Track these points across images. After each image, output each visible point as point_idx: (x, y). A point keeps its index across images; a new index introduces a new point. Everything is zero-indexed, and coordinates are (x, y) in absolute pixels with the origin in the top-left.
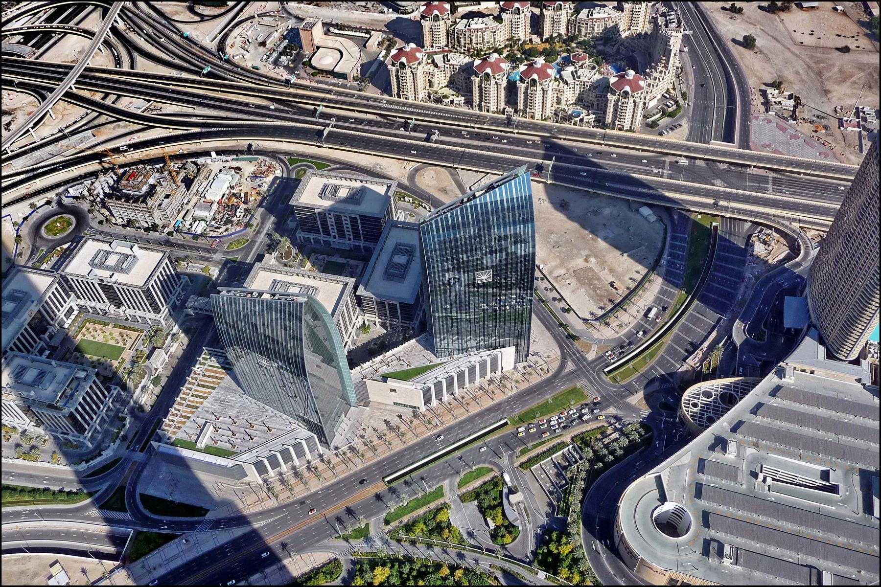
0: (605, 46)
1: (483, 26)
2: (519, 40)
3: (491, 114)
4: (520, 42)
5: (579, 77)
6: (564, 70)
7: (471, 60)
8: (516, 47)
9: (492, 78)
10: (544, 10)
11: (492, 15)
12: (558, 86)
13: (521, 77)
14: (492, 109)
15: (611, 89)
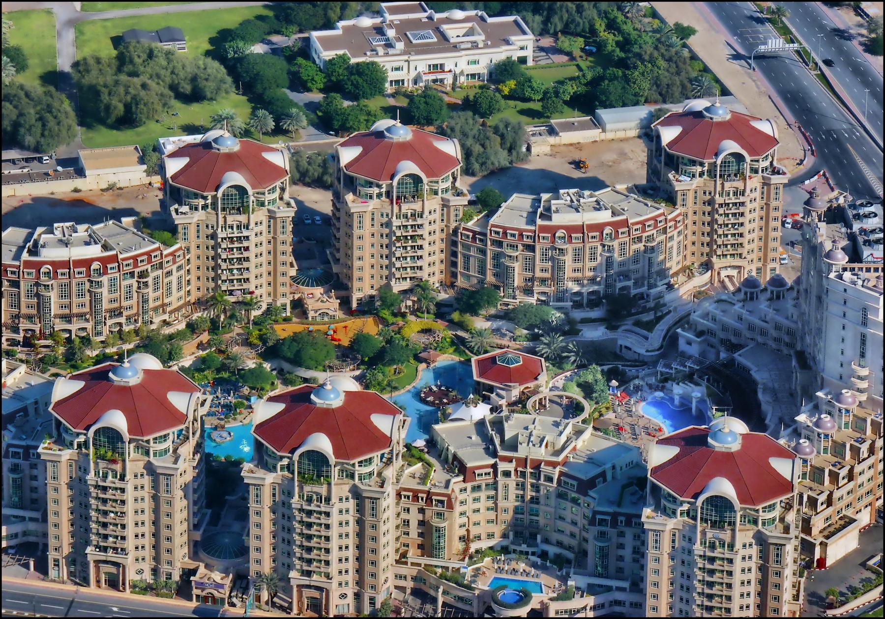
0: (612, 327)
1: (95, 251)
2: (248, 305)
3: (128, 595)
4: (255, 313)
5: (513, 446)
6: (446, 417)
7: (37, 380)
8: (237, 329)
9: (131, 451)
10: (350, 197)
11: (129, 212)
12: (424, 478)
13: (258, 446)
14: (131, 575)
15: (655, 489)
